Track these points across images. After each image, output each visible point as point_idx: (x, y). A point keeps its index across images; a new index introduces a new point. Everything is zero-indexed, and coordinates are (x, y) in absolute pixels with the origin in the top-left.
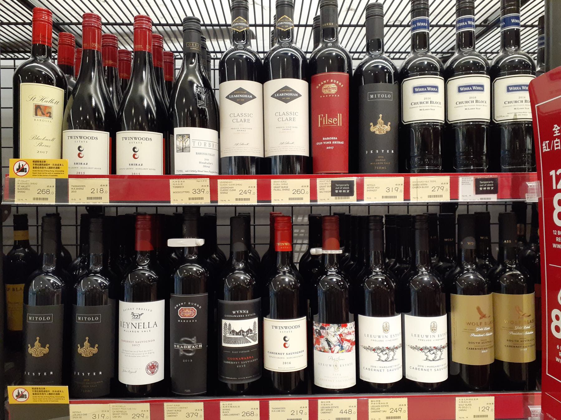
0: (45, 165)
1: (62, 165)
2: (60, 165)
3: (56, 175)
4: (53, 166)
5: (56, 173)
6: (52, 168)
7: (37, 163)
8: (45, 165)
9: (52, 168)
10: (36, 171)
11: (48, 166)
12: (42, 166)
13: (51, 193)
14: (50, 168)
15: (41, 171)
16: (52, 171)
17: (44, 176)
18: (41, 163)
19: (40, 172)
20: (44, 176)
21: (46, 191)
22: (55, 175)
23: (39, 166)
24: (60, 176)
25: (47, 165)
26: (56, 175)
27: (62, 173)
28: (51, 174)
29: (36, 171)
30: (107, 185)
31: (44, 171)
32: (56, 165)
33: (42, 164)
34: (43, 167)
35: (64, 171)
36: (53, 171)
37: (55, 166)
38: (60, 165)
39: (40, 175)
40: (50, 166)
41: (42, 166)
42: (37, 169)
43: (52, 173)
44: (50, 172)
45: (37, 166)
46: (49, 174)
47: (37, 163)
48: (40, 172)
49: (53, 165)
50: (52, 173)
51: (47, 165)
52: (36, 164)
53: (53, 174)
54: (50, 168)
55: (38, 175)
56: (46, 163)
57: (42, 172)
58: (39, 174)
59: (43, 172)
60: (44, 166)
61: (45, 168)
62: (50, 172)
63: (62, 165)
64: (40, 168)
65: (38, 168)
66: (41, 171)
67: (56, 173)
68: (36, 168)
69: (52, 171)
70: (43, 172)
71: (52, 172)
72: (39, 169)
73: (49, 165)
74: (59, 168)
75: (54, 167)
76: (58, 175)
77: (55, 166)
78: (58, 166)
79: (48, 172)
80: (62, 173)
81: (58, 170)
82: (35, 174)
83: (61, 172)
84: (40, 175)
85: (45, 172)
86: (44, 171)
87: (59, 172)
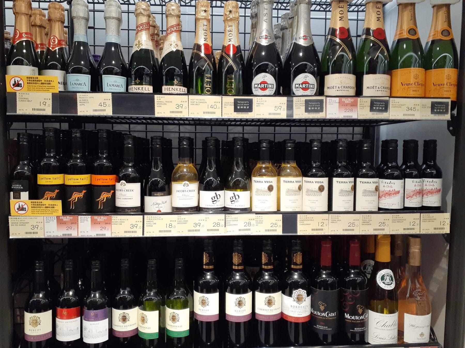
2: (55, 205)
3: (52, 213)
4: (49, 206)
5: (52, 212)
6: (48, 207)
7: (35, 204)
11: (45, 206)
12: (39, 206)
16: (48, 210)
19: (39, 211)
22: (51, 213)
23: (37, 206)
25: (43, 205)
31: (41, 210)
32: (51, 205)
34: (40, 207)
35: (58, 210)
37: (51, 206)
39: (38, 213)
40: (46, 206)
41: (39, 206)
42: (34, 209)
43: (48, 212)
44: (46, 211)
45: (35, 206)
46: (45, 213)
47: (35, 204)
48: (39, 211)
49: (49, 205)
50: (48, 212)
51: (43, 205)
52: (34, 205)
53: (49, 213)
54: (46, 207)
55: (36, 214)
56: (42, 204)
57: (39, 211)
58: (37, 213)
60: (41, 206)
61: (42, 207)
62: (46, 211)
63: (56, 205)
64: (38, 207)
65: (36, 207)
68: (34, 207)
69: (48, 210)
70: (41, 211)
73: (45, 205)
74: (54, 207)
75: (50, 207)
76: (53, 213)
77: (51, 206)
78: (53, 206)
79: (44, 211)
81: (53, 209)
83: (56, 211)
84: (38, 213)
85: (42, 211)
87: (54, 211)
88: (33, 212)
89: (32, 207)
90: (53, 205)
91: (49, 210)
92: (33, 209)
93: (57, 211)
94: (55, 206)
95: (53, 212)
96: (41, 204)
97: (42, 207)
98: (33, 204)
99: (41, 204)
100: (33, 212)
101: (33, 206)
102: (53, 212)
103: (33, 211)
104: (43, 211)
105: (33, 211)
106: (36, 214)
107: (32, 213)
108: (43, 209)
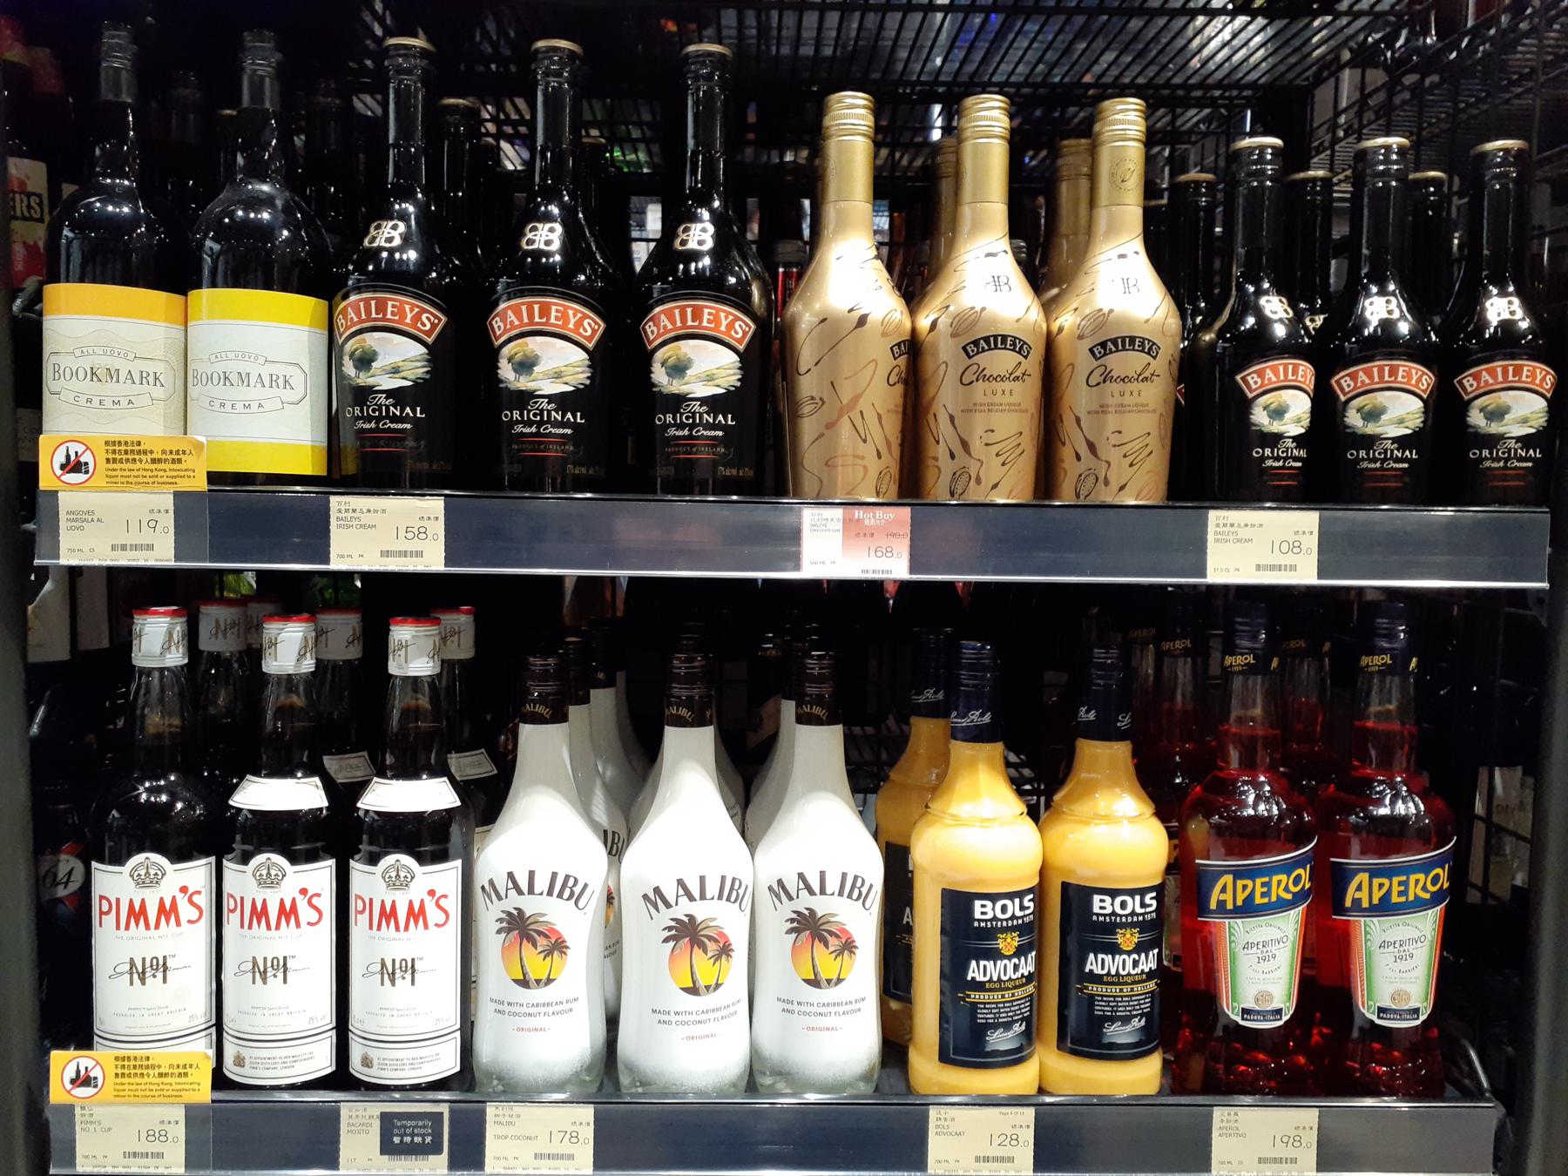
0: (139, 452)
1: (188, 452)
2: (184, 452)
3: (174, 480)
4: (164, 457)
5: (172, 477)
6: (159, 461)
8: (139, 452)
9: (159, 461)
10: (115, 470)
11: (149, 457)
12: (130, 457)
13: (430, 536)
14: (154, 461)
15: (130, 470)
17: (139, 483)
18: (129, 448)
19: (127, 473)
20: (139, 483)
21: (417, 533)
22: (170, 480)
23: (124, 457)
24: (186, 485)
25: (145, 452)
26: (174, 480)
27: (189, 477)
28: (161, 480)
29: (115, 470)
30: (437, 518)
31: (138, 470)
33: (132, 451)
34: (134, 460)
36: (165, 471)
37: (170, 457)
38: (184, 452)
39: (128, 482)
40: (153, 456)
41: (130, 457)
42: (115, 466)
44: (155, 473)
47: (117, 448)
48: (127, 473)
49: (164, 452)
51: (145, 452)
52: (114, 452)
54: (154, 461)
56: (141, 448)
57: (132, 473)
58: (124, 480)
59: (136, 473)
60: (137, 457)
61: (141, 461)
62: (155, 473)
64: (127, 460)
65: (121, 461)
66: (130, 470)
67: (172, 477)
68: (114, 460)
70: (136, 473)
71: (162, 473)
72: (124, 466)
73: (151, 452)
74: (179, 461)
75: (166, 460)
76: (177, 480)
77: (170, 457)
78: (176, 457)
80: (189, 477)
82: (113, 480)
83: (186, 473)
84: (128, 482)
86: (138, 470)
88: (110, 477)
89: (108, 460)
90: (178, 452)
91: (165, 471)
92: (111, 466)
93: (190, 473)
94: (182, 456)
95: (175, 477)
96: (137, 448)
97: (141, 461)
98: (111, 448)
99: (138, 448)
100: (110, 477)
101: (111, 456)
102: (175, 477)
103: (110, 473)
104: (145, 473)
105: (110, 473)
106: (122, 483)
107: (108, 480)
108: (143, 466)
